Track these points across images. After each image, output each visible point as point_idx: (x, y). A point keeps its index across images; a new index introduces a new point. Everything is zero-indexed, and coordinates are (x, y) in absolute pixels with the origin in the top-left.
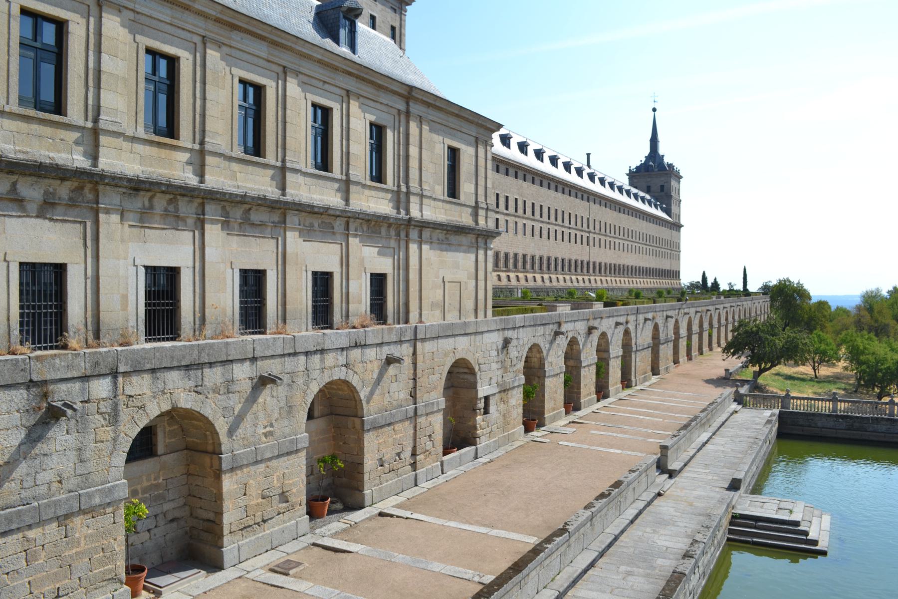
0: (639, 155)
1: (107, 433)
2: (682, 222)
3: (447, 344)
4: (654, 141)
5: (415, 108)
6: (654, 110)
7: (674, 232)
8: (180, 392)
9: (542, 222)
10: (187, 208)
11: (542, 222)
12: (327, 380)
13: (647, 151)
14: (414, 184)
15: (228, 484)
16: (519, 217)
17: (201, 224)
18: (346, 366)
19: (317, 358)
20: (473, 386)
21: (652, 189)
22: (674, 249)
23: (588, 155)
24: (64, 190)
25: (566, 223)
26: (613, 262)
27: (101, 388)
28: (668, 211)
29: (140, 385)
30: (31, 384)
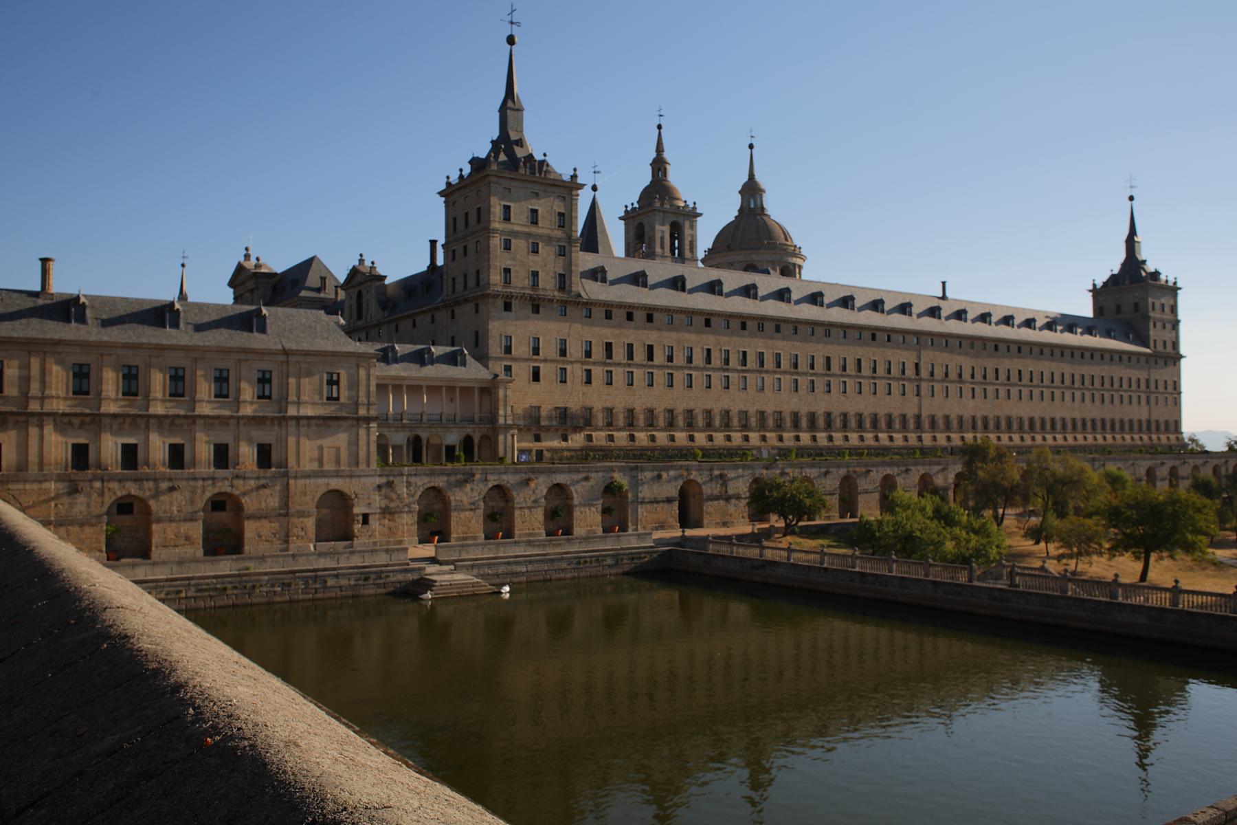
0: (1113, 262)
1: (100, 500)
2: (1183, 351)
3: (322, 481)
4: (1131, 242)
5: (291, 358)
8: (133, 489)
10: (139, 421)
12: (216, 491)
13: (1122, 256)
14: (292, 398)
15: (154, 527)
16: (767, 372)
17: (147, 428)
18: (232, 486)
19: (210, 482)
20: (353, 506)
23: (944, 283)
24: (88, 419)
27: (98, 485)
28: (1143, 341)
29: (114, 485)
30: (70, 481)
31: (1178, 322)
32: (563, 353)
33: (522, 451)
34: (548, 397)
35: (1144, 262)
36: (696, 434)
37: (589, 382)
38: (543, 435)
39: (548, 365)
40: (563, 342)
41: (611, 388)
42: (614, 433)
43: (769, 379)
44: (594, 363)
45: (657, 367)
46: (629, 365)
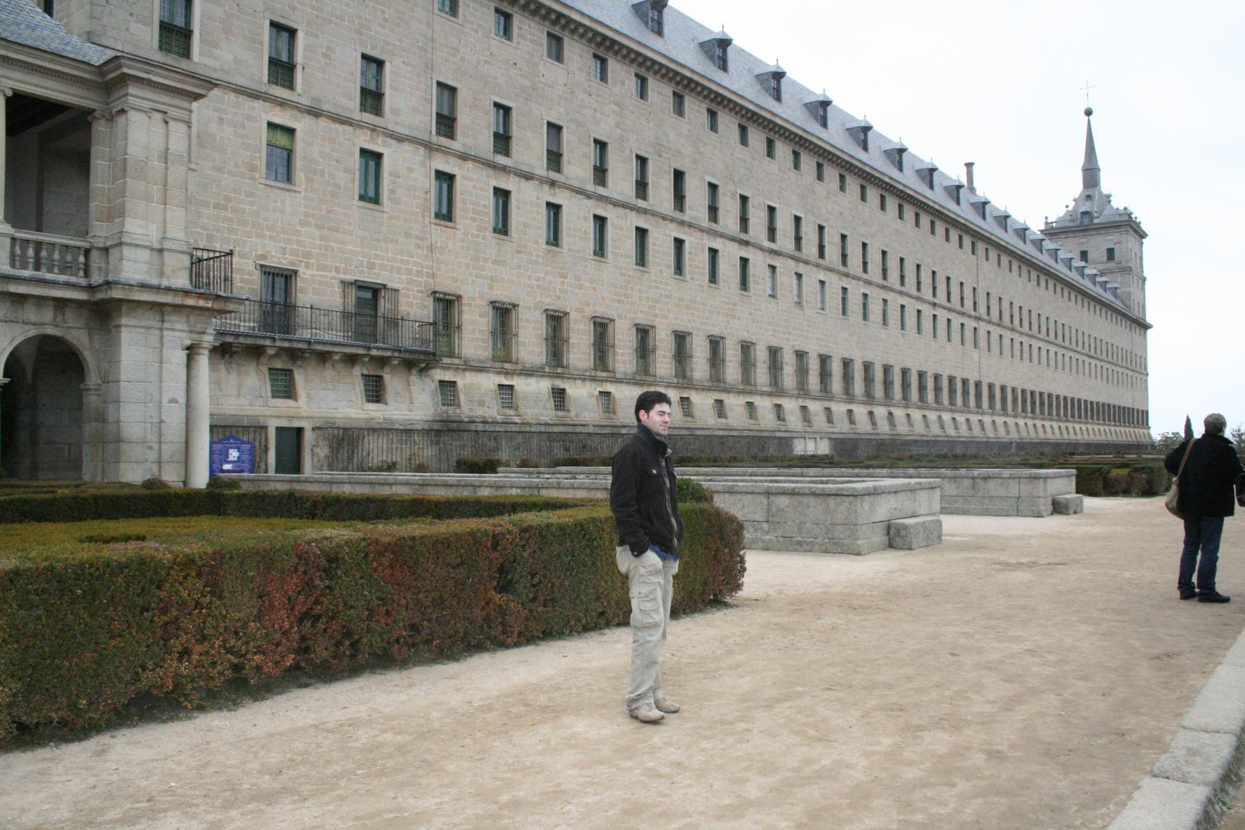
6: (1088, 113)
7: (1136, 336)
9: (868, 283)
11: (868, 283)
13: (1076, 187)
21: (1090, 257)
22: (1136, 368)
23: (969, 166)
25: (927, 292)
26: (1029, 387)
31: (1144, 280)
32: (372, 98)
33: (224, 432)
34: (323, 242)
35: (1109, 196)
36: (695, 398)
37: (446, 214)
38: (299, 378)
39: (323, 123)
40: (374, 63)
41: (508, 246)
42: (520, 384)
43: (812, 277)
44: (464, 157)
45: (616, 204)
46: (553, 184)
